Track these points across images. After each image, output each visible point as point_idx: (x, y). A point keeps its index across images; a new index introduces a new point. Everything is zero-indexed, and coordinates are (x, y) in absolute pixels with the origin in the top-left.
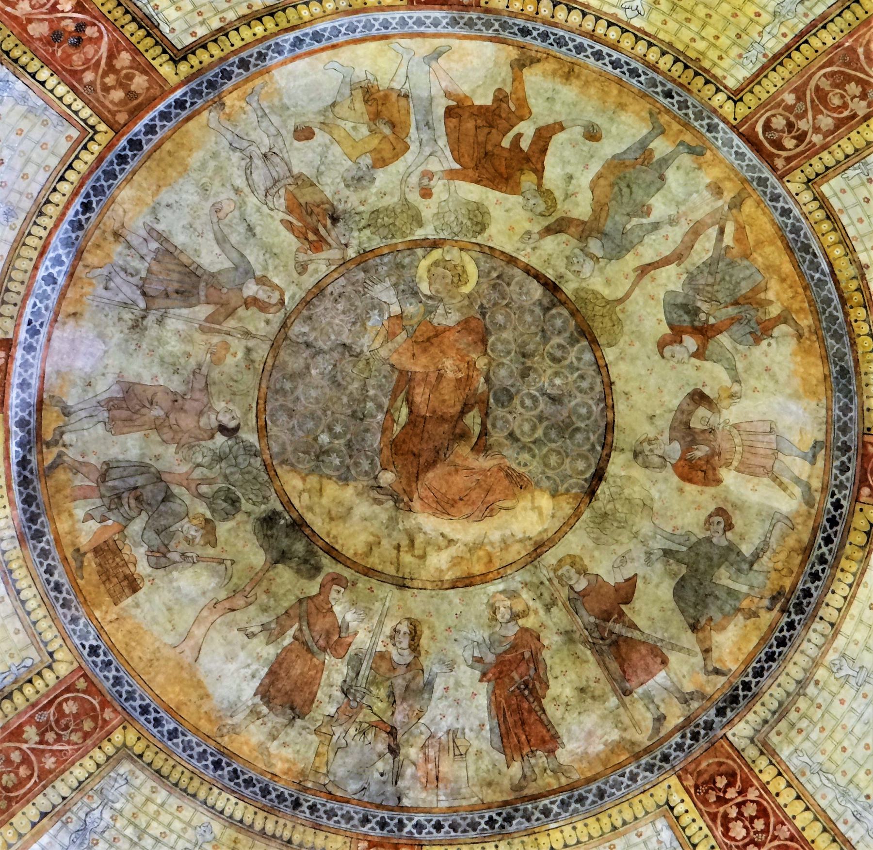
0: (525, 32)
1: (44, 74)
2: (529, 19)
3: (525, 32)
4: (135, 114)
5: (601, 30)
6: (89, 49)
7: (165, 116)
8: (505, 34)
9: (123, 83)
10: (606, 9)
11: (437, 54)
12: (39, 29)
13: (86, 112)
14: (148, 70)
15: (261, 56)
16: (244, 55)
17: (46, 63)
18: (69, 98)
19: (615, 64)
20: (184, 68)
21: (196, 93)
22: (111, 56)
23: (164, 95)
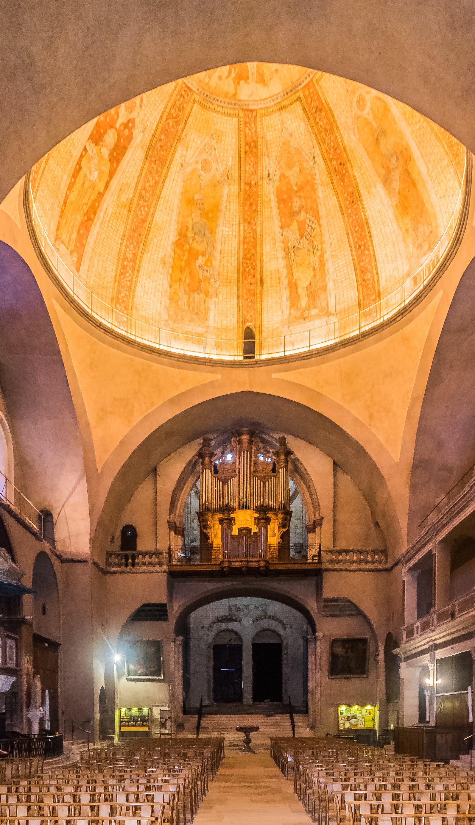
0: (235, 104)
1: (324, 101)
2: (234, 109)
3: (235, 104)
4: (308, 84)
5: (221, 109)
6: (315, 106)
7: (303, 81)
8: (239, 102)
9: (310, 93)
10: (220, 116)
11: (251, 95)
12: (323, 114)
13: (317, 88)
14: (305, 96)
15: (284, 95)
16: (287, 96)
17: (323, 104)
18: (320, 93)
19: (218, 100)
20: (298, 95)
21: (296, 87)
22: (311, 102)
23: (303, 88)
